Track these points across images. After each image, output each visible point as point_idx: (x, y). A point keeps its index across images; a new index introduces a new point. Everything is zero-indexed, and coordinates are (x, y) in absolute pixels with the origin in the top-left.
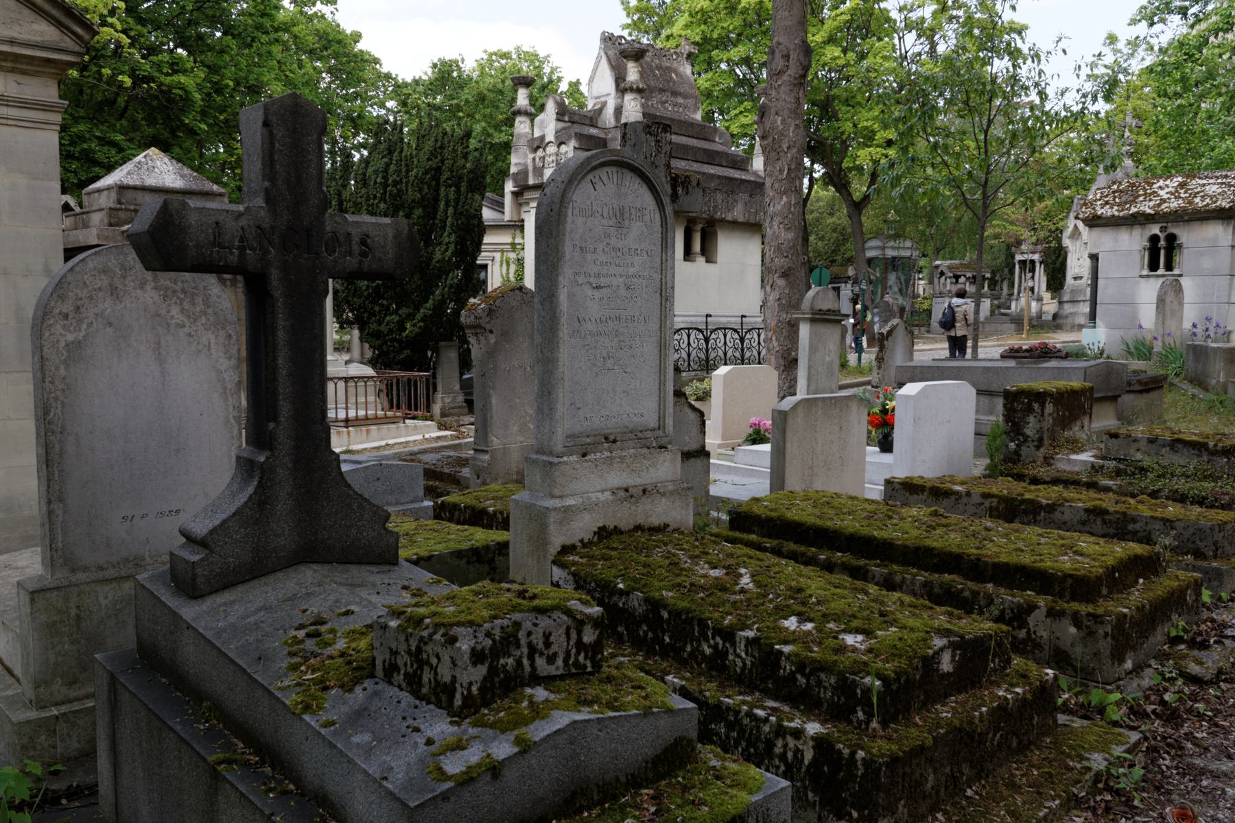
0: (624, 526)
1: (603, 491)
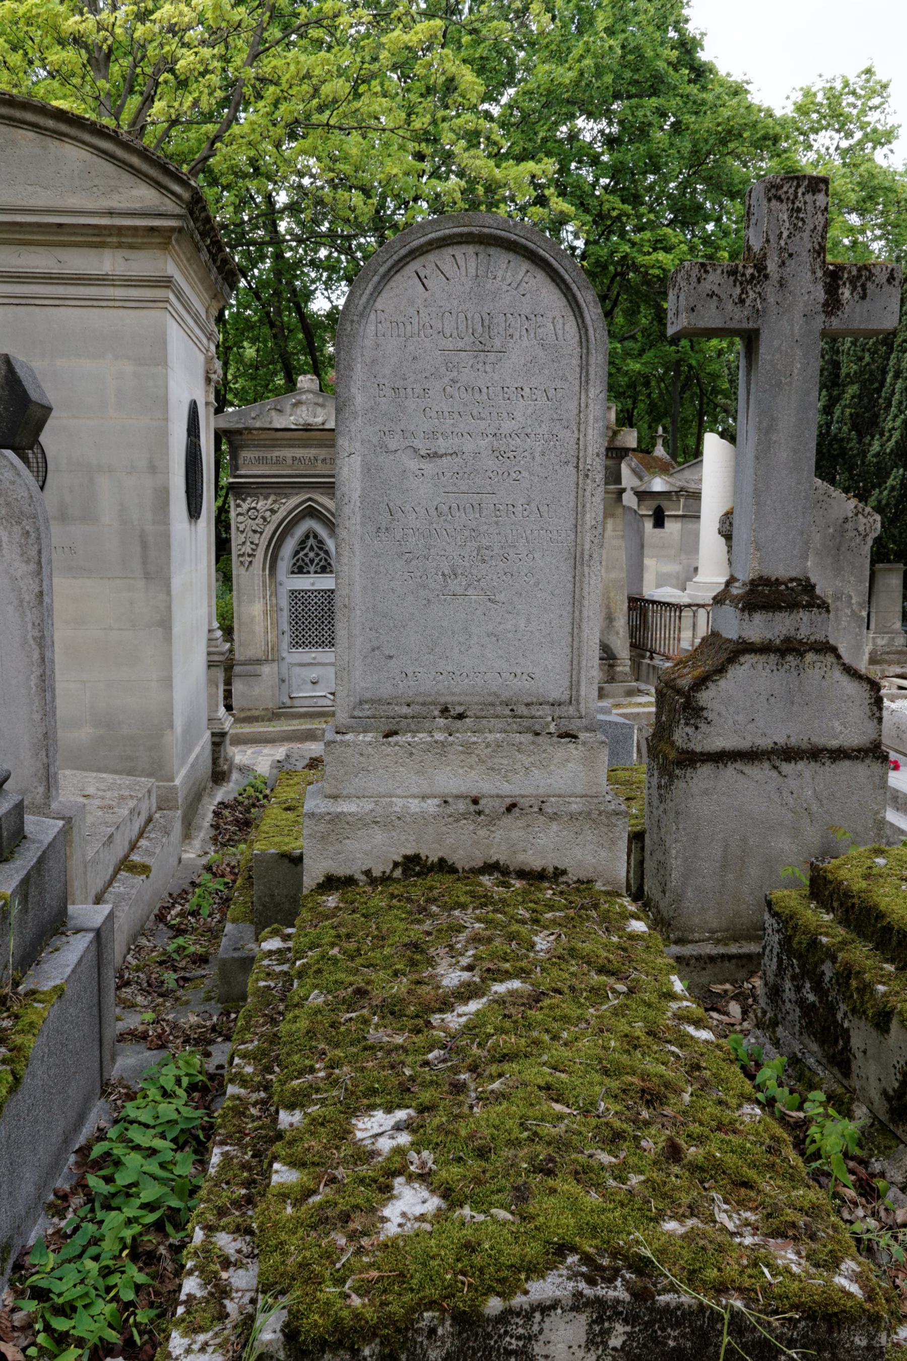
0: (460, 859)
1: (424, 797)
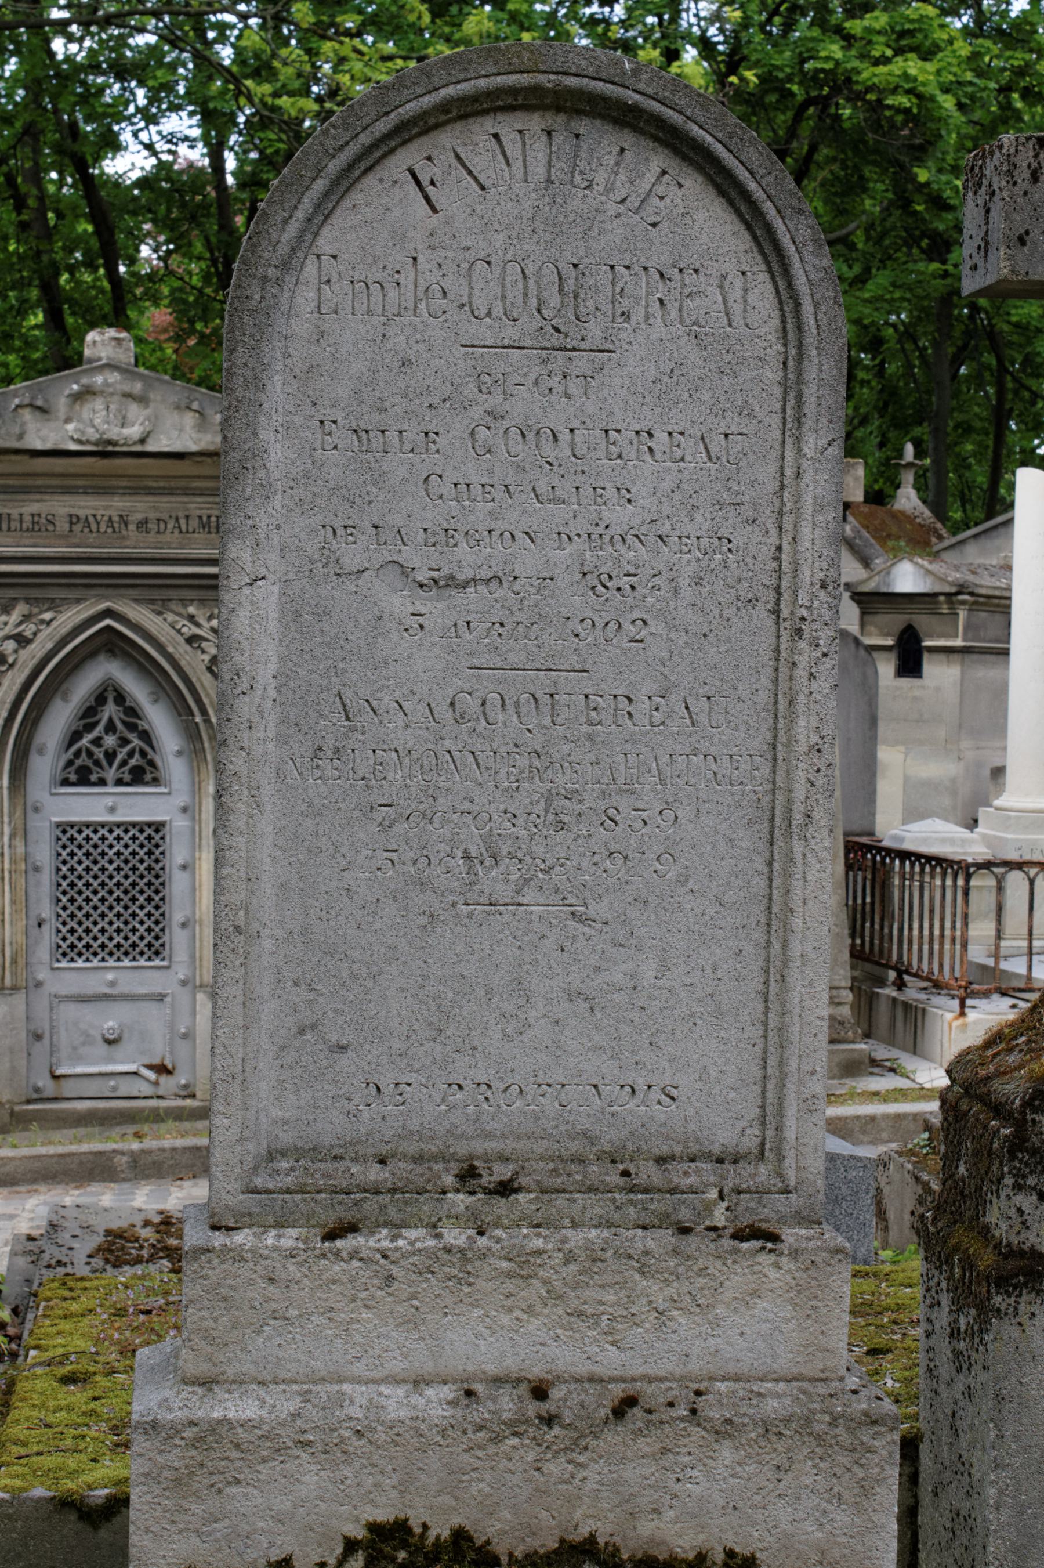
1: (418, 1383)
